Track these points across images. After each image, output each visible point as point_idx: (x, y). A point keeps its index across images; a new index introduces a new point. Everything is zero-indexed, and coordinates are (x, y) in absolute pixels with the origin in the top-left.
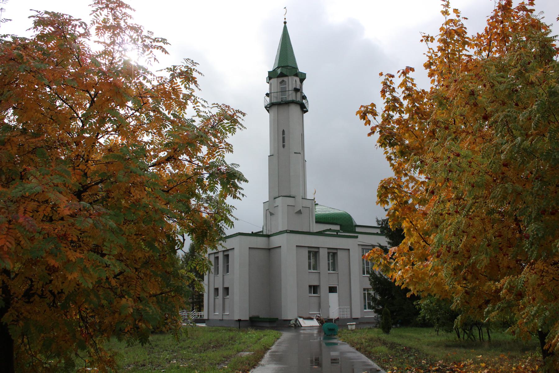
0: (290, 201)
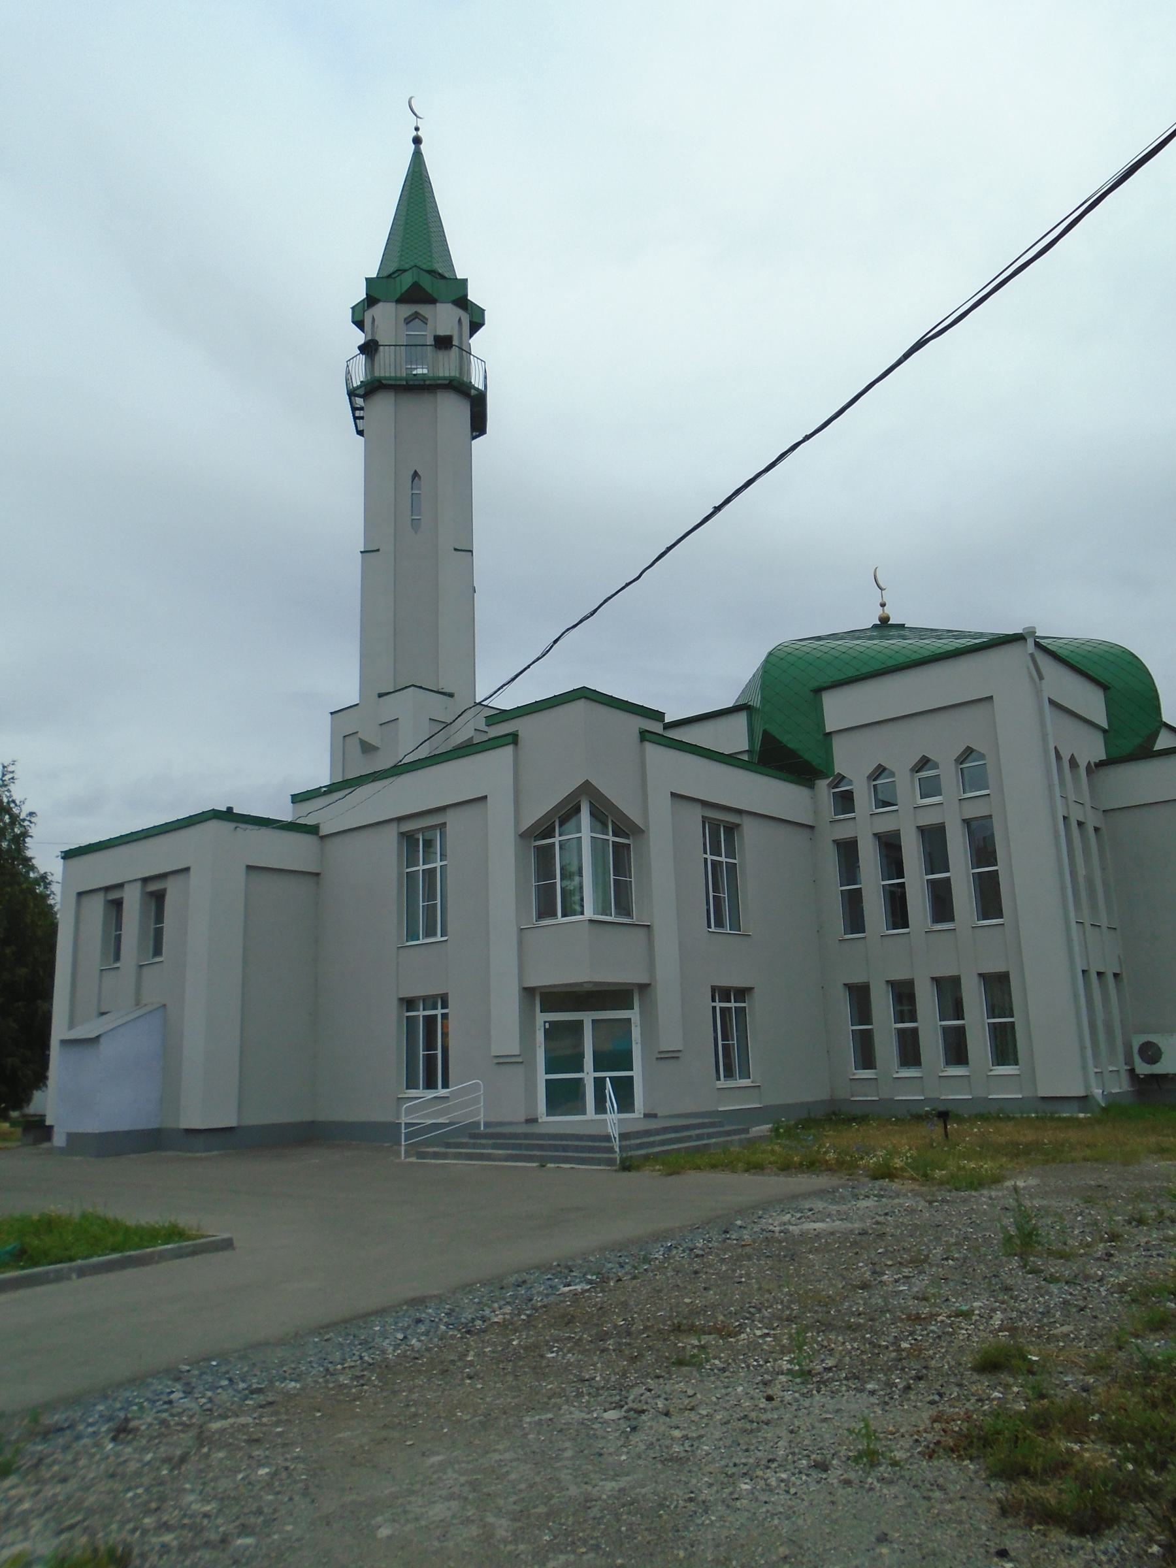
0: (439, 708)
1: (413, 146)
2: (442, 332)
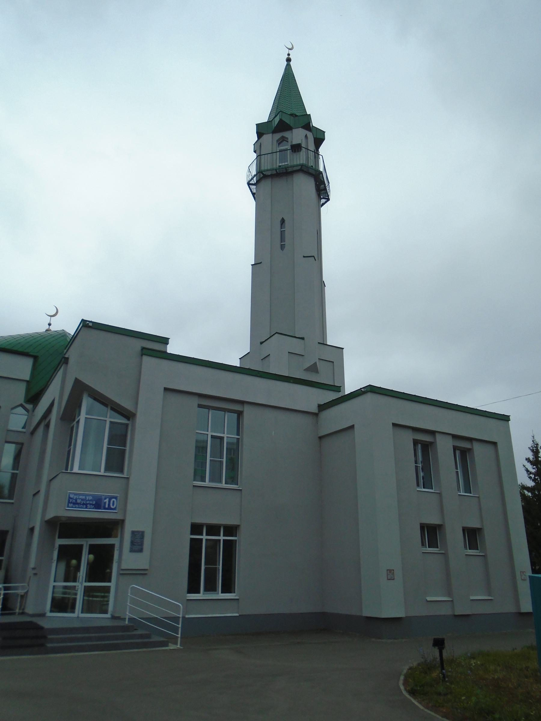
1: (286, 63)
2: (294, 143)
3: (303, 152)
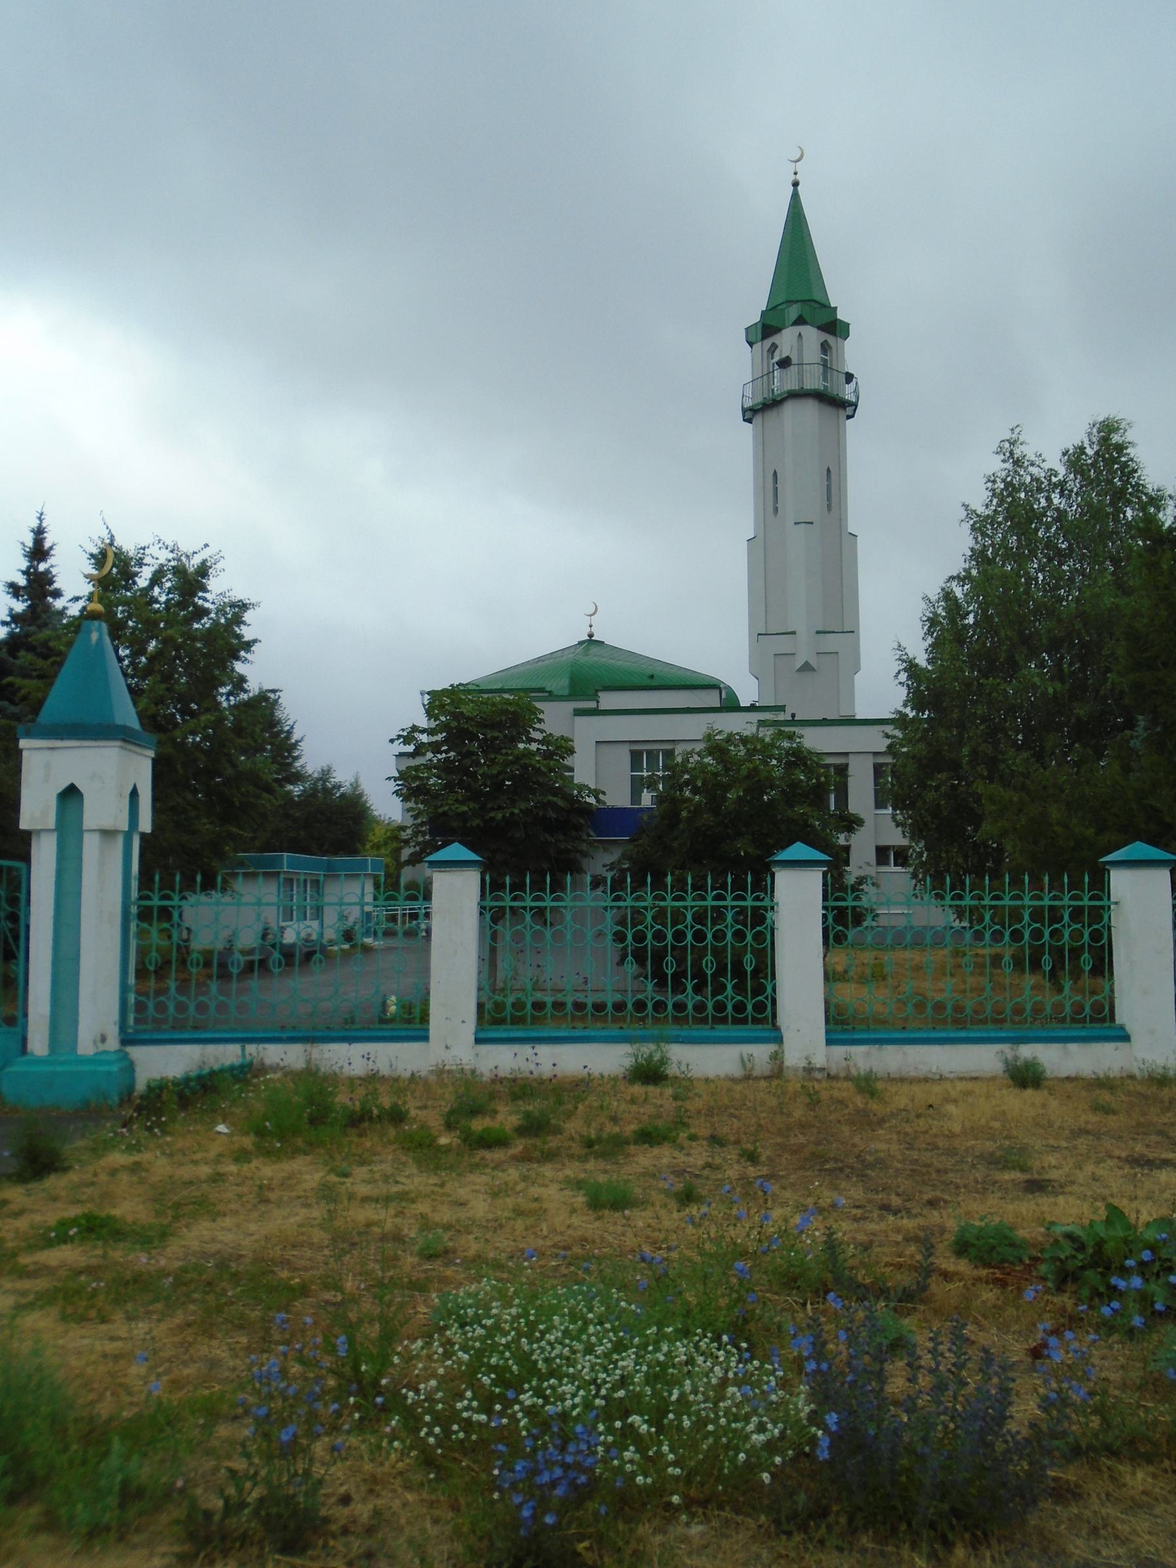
3: (793, 369)
